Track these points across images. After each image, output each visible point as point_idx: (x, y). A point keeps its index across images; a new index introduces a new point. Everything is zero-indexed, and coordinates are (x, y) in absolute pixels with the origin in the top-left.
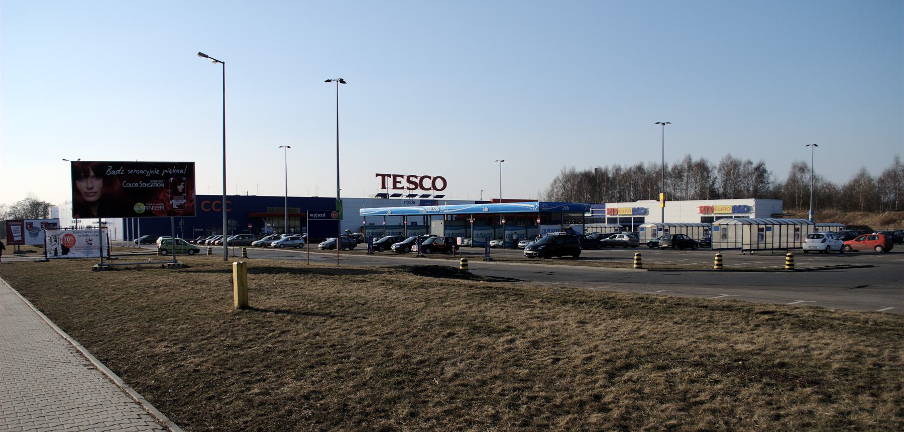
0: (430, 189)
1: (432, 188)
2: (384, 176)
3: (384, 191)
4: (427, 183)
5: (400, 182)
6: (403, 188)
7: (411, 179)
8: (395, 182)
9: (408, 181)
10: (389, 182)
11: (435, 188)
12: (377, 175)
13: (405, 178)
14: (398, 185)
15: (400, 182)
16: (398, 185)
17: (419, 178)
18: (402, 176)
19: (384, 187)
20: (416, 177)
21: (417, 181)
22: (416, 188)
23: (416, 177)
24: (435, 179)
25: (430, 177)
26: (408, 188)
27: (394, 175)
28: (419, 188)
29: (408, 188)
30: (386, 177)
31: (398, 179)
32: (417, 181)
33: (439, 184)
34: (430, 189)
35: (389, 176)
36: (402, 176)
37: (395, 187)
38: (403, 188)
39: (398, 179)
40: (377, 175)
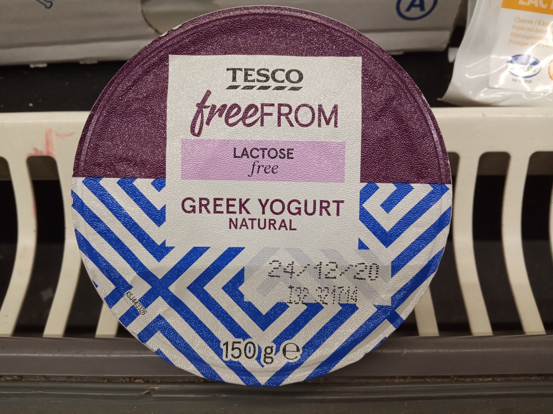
0: (283, 82)
1: (286, 81)
2: (234, 71)
3: (234, 84)
4: (280, 76)
5: (251, 75)
6: (253, 81)
7: (263, 72)
8: (246, 75)
9: (259, 74)
10: (240, 75)
12: (228, 70)
13: (256, 71)
14: (249, 78)
15: (251, 75)
16: (249, 78)
18: (253, 70)
19: (234, 79)
20: (268, 70)
21: (269, 74)
22: (267, 81)
23: (268, 70)
24: (289, 72)
25: (283, 70)
26: (258, 81)
28: (271, 79)
29: (258, 81)
30: (237, 71)
31: (250, 72)
32: (269, 74)
33: (294, 76)
34: (283, 82)
35: (241, 70)
36: (253, 70)
37: (246, 80)
38: (253, 81)
39: (250, 72)
40: (228, 70)
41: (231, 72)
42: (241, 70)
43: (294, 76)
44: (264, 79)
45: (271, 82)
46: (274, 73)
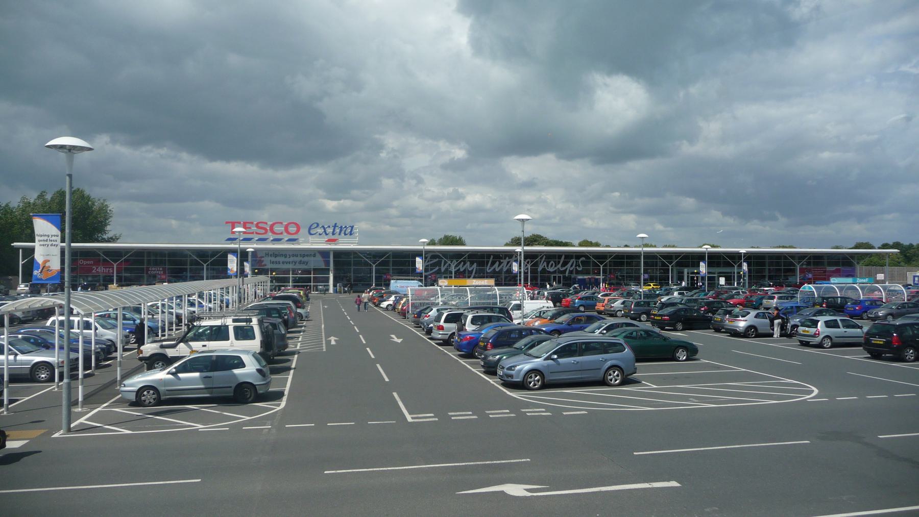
0: (282, 233)
4: (277, 228)
6: (253, 233)
7: (260, 225)
9: (257, 226)
11: (288, 233)
12: (227, 223)
17: (270, 223)
18: (252, 223)
20: (266, 223)
25: (281, 223)
26: (257, 233)
27: (244, 222)
29: (257, 233)
33: (292, 229)
34: (282, 233)
35: (239, 223)
36: (252, 223)
38: (253, 233)
40: (227, 223)
41: (231, 224)
42: (239, 223)
43: (292, 229)
44: (263, 231)
45: (271, 236)
46: (272, 227)
